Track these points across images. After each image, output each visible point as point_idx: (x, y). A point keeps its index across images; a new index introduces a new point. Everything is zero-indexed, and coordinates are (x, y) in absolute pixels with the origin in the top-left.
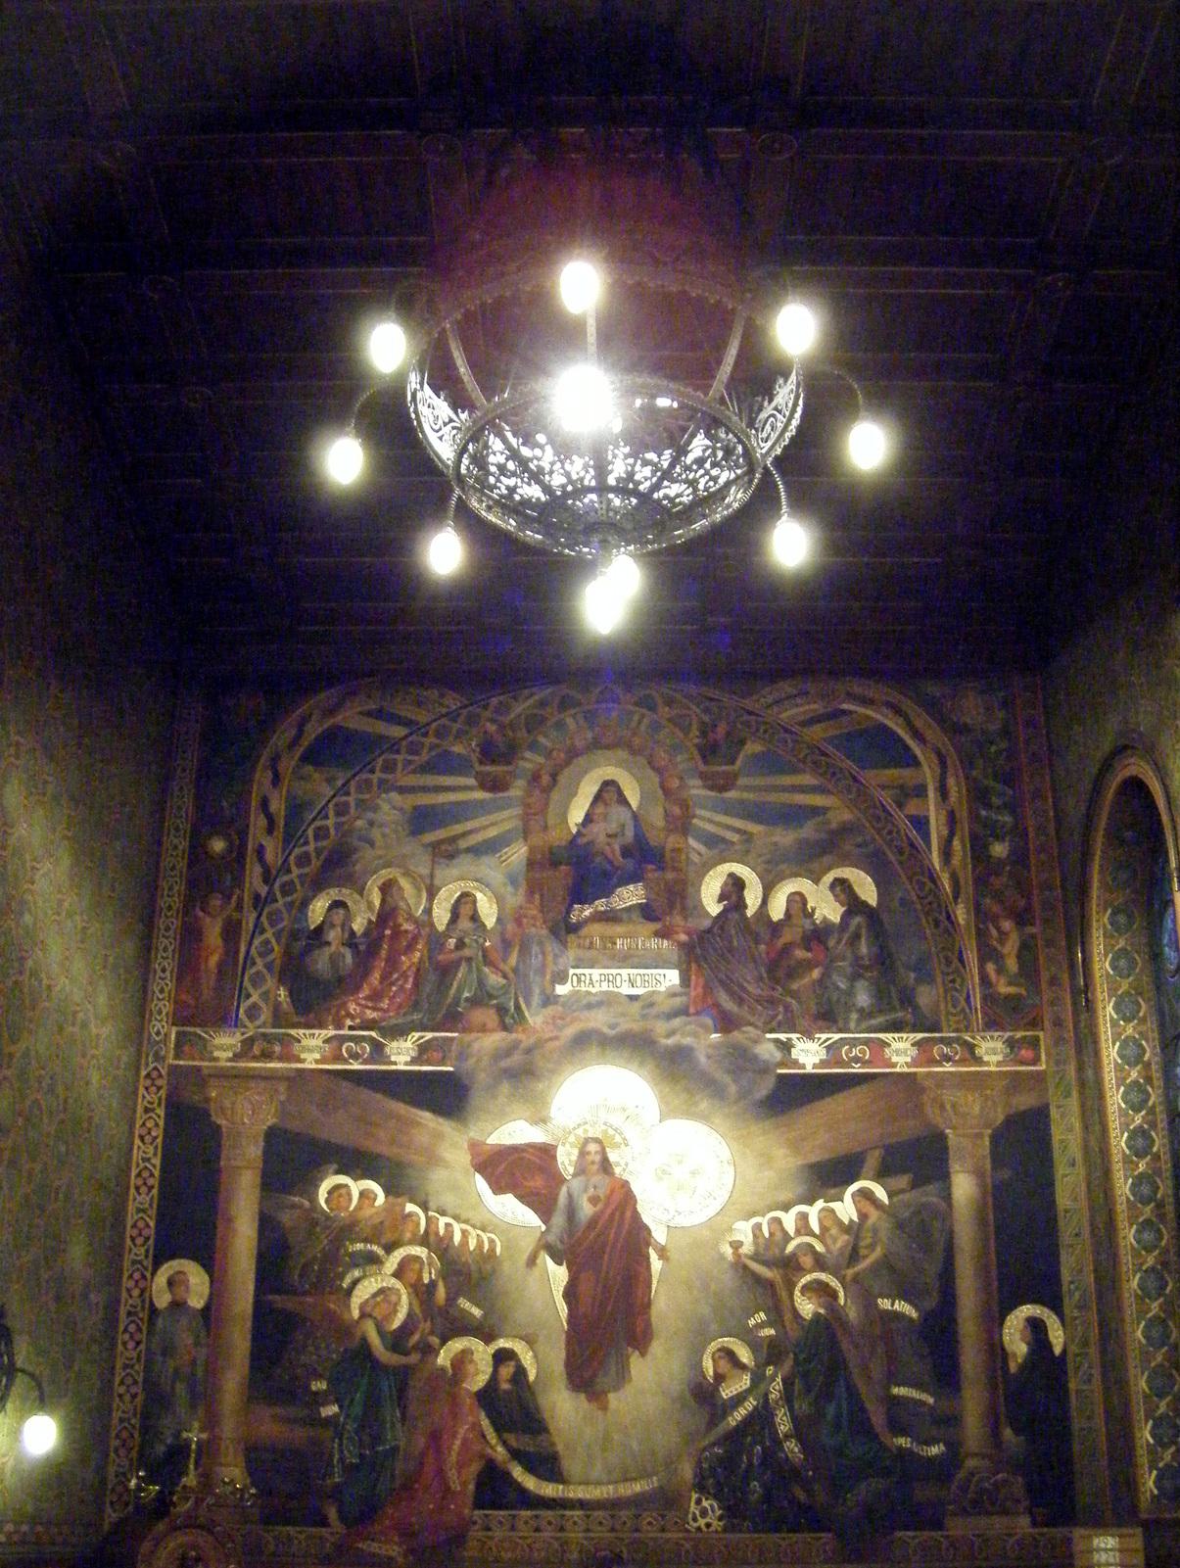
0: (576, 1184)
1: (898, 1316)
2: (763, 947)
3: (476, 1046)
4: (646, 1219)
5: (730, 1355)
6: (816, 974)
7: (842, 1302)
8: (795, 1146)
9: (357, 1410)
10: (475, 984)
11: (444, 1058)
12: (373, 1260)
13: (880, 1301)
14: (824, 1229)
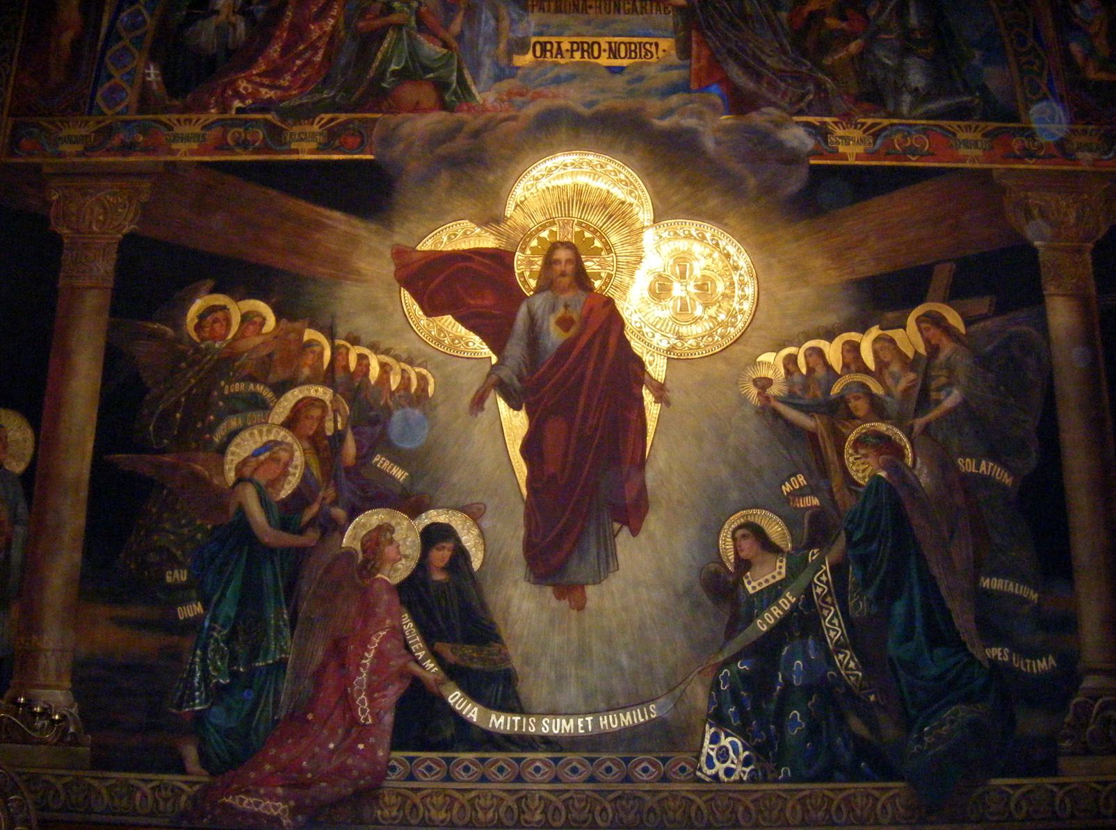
0: (540, 303)
1: (986, 480)
2: (784, 15)
3: (406, 128)
4: (637, 347)
5: (757, 532)
6: (854, 47)
7: (909, 462)
8: (838, 256)
9: (229, 609)
10: (405, 55)
11: (362, 142)
12: (261, 406)
13: (960, 461)
14: (881, 364)
